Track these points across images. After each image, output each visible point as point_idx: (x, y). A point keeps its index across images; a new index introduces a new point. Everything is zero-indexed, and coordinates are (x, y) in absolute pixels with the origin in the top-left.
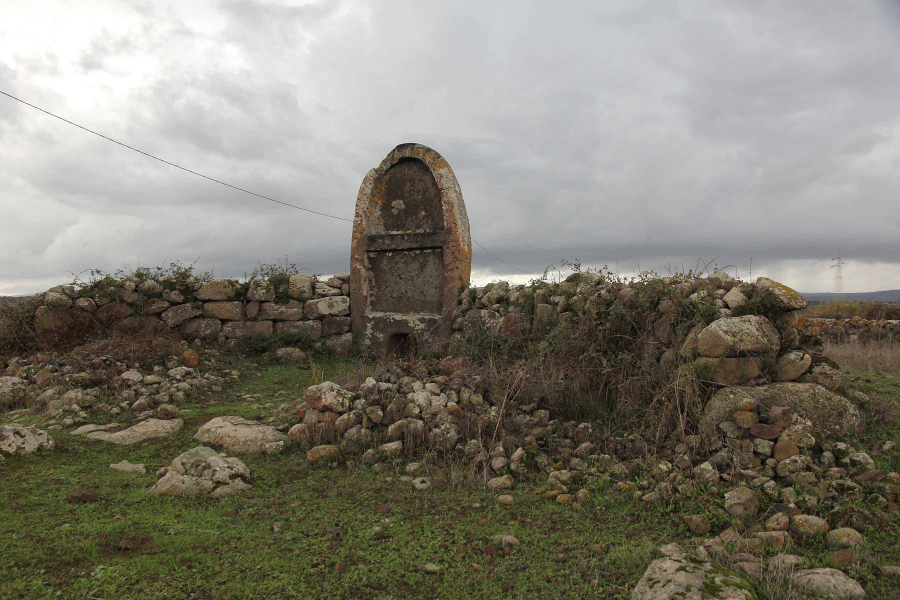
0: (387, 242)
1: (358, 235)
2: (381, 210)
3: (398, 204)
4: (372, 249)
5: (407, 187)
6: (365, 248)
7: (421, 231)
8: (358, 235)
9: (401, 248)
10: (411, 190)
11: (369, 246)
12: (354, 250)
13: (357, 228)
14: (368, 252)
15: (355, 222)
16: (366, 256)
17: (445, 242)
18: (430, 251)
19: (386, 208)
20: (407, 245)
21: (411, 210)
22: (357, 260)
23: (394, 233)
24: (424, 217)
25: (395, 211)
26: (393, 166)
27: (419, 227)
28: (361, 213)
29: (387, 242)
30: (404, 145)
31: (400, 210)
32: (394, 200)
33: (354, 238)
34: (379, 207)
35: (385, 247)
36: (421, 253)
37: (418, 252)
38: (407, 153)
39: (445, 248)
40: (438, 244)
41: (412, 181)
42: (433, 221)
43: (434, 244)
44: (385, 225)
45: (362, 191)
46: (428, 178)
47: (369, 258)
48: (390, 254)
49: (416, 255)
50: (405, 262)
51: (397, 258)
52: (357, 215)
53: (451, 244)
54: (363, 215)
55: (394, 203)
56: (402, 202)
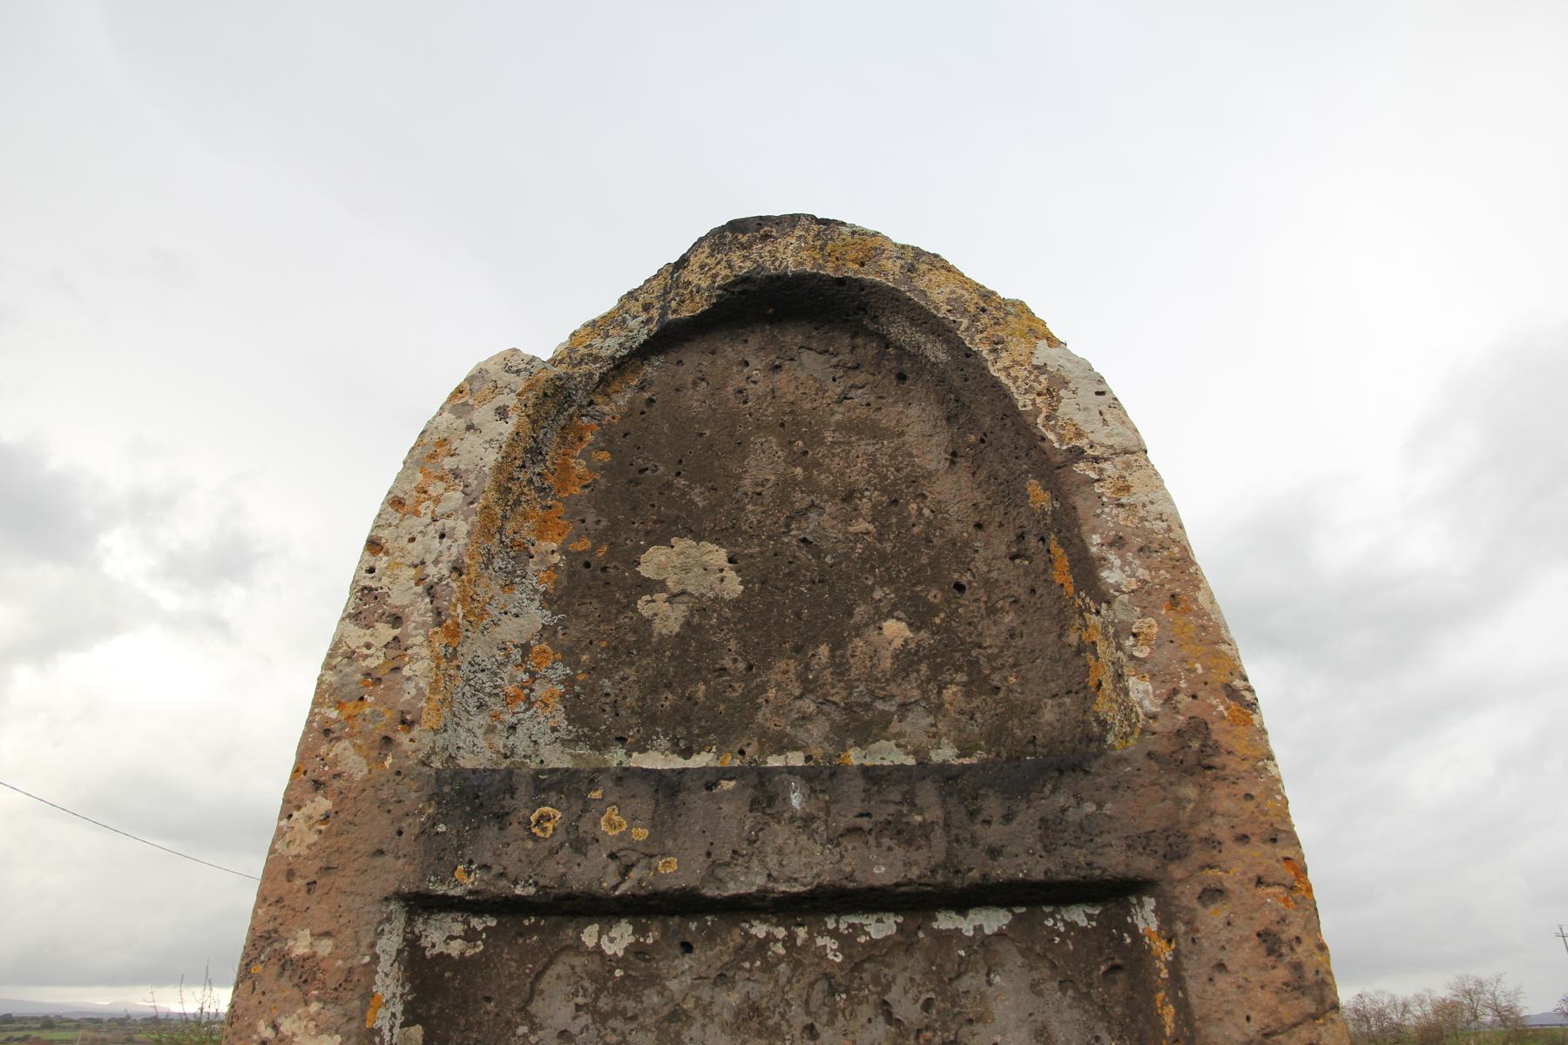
0: (611, 824)
1: (351, 759)
2: (548, 600)
3: (689, 572)
4: (464, 883)
5: (764, 464)
6: (398, 873)
7: (886, 754)
8: (351, 759)
9: (744, 882)
10: (786, 485)
11: (439, 854)
12: (287, 886)
13: (349, 700)
14: (421, 904)
15: (340, 655)
16: (390, 944)
17: (1173, 844)
18: (993, 920)
19: (596, 588)
20: (802, 863)
21: (795, 606)
22: (303, 973)
23: (656, 760)
24: (907, 660)
25: (666, 617)
26: (670, 338)
27: (864, 729)
28: (402, 592)
29: (611, 824)
30: (761, 221)
31: (702, 608)
32: (663, 540)
33: (310, 776)
34: (537, 576)
35: (592, 873)
36: (904, 942)
37: (880, 927)
38: (790, 257)
39: (1187, 895)
40: (1114, 861)
41: (796, 430)
42: (977, 684)
43: (1075, 860)
44: (586, 718)
45: (430, 453)
46: (918, 427)
47: (420, 968)
48: (619, 939)
49: (863, 957)
50: (751, 1013)
51: (681, 975)
52: (367, 602)
53: (1236, 866)
54: (420, 612)
55: (654, 561)
56: (717, 556)
